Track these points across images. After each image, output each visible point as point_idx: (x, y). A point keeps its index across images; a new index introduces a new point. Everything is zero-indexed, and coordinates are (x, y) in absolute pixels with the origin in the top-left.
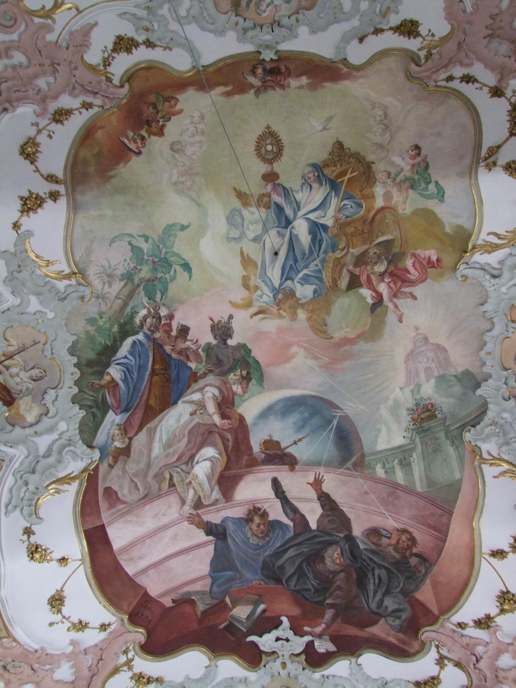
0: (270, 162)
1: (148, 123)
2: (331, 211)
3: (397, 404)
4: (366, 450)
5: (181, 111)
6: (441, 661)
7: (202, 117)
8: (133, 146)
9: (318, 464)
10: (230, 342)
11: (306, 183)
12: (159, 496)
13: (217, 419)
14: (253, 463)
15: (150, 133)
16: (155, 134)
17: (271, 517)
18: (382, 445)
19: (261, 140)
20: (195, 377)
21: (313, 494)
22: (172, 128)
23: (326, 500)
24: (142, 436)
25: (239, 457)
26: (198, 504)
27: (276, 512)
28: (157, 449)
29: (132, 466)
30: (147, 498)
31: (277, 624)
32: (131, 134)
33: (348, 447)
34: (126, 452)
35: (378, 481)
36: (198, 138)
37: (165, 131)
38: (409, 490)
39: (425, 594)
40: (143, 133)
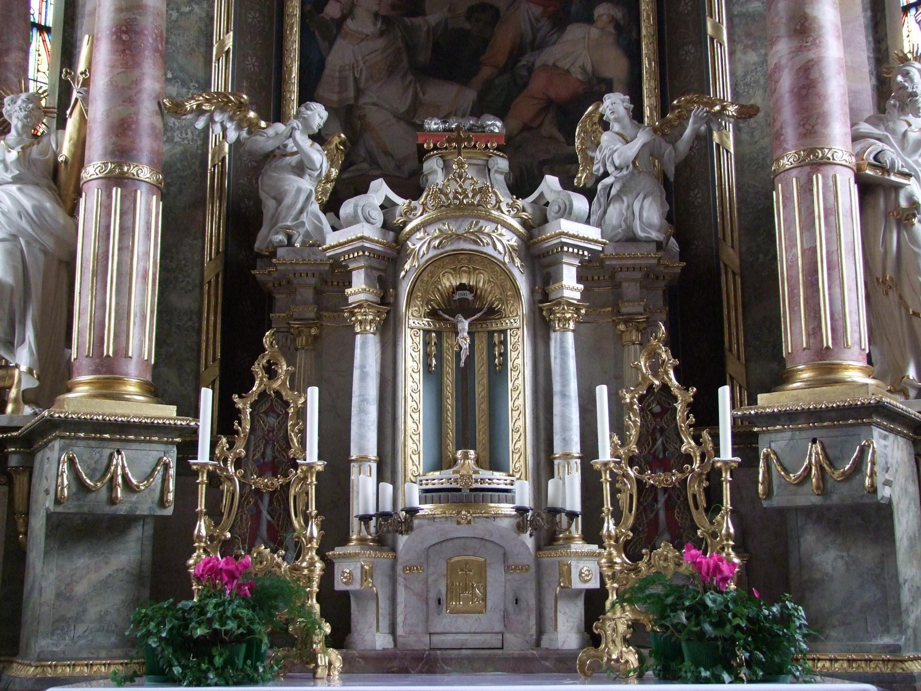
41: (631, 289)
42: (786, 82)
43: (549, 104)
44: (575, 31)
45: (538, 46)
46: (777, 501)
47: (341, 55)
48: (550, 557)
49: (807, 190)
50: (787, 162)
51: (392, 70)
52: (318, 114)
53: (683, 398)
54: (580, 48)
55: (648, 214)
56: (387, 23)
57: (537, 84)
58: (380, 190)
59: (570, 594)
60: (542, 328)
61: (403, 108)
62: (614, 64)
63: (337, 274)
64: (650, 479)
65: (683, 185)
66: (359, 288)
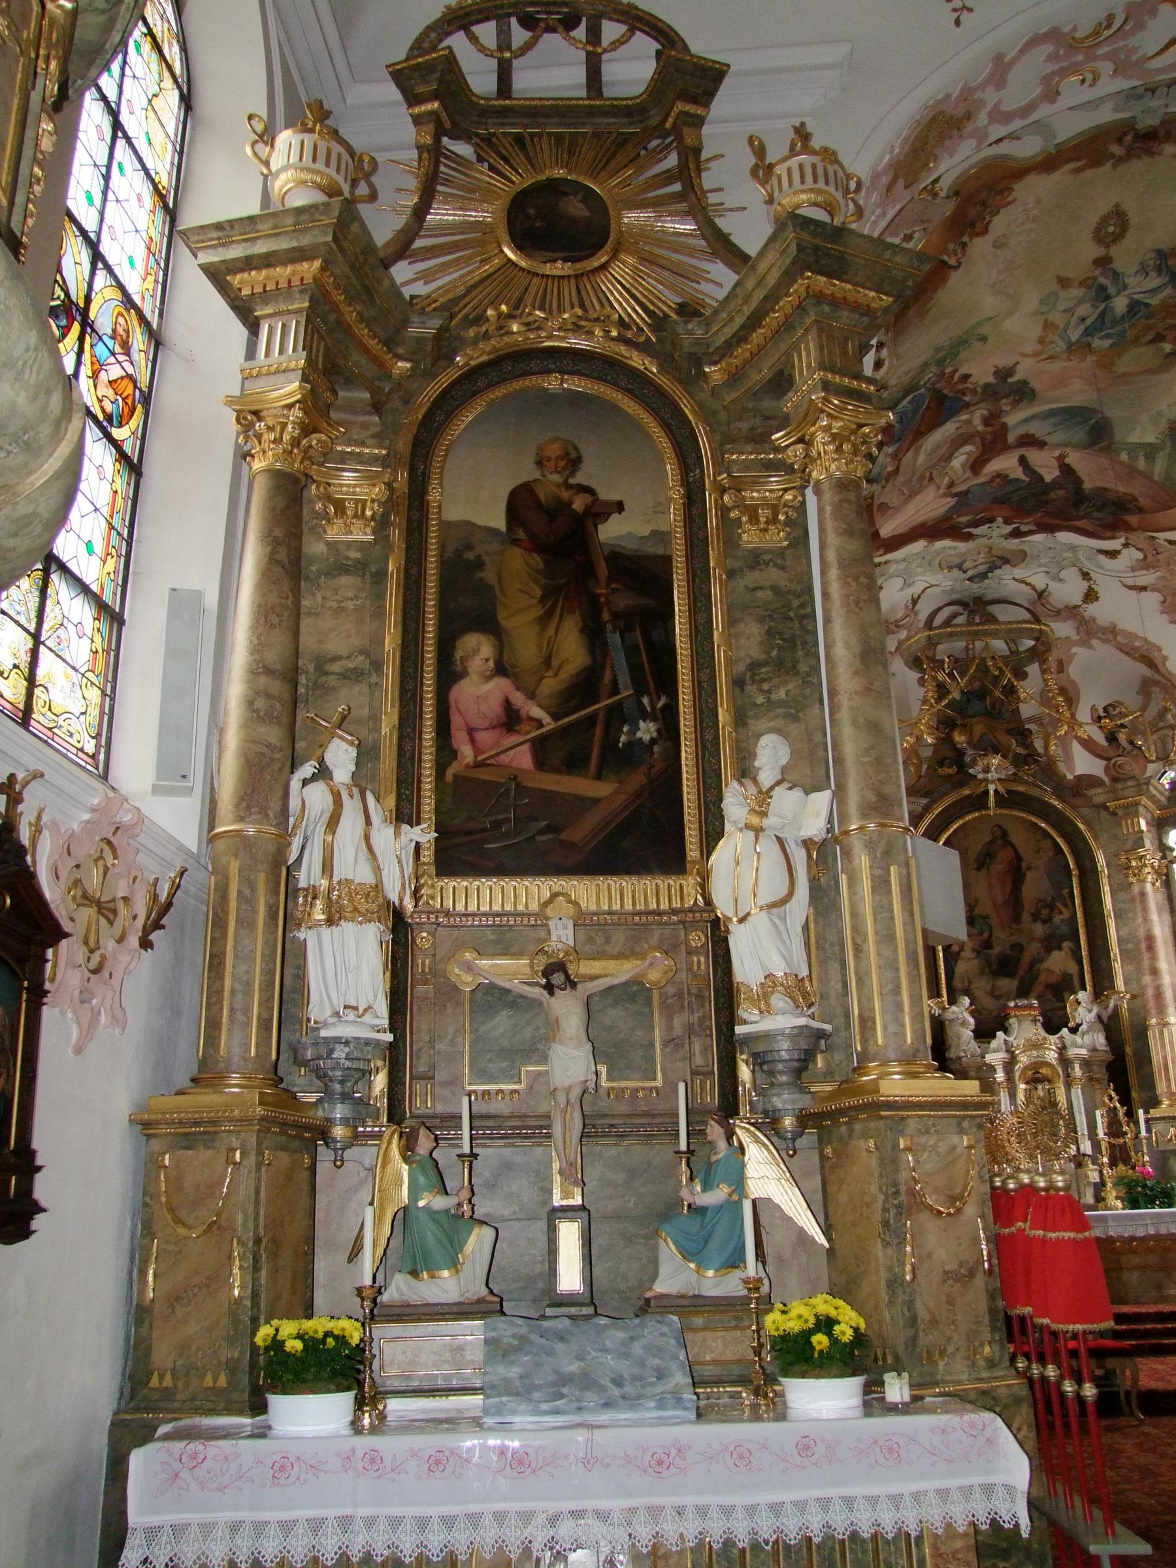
0: (1107, 246)
1: (972, 225)
2: (1161, 296)
3: (1160, 414)
4: (1117, 437)
5: (1014, 200)
6: (1126, 545)
7: (1038, 201)
8: (952, 261)
9: (1066, 445)
10: (1010, 380)
11: (1143, 270)
12: (920, 491)
13: (980, 428)
14: (1006, 448)
15: (972, 236)
16: (978, 235)
17: (1012, 476)
18: (1134, 438)
19: (1105, 220)
20: (967, 405)
21: (1055, 463)
22: (999, 224)
23: (1066, 470)
24: (910, 454)
25: (994, 442)
26: (952, 484)
27: (1018, 473)
28: (922, 458)
29: (900, 479)
30: (913, 494)
31: (991, 520)
32: (951, 246)
33: (1099, 433)
34: (896, 471)
35: (1122, 464)
36: (1027, 226)
37: (991, 227)
38: (1147, 477)
39: (1133, 520)
40: (965, 239)
41: (1095, 1068)
42: (1150, 992)
43: (1049, 986)
44: (1055, 954)
45: (1041, 961)
46: (1161, 1148)
47: (961, 967)
48: (1080, 1171)
49: (1162, 1033)
50: (1153, 1021)
51: (982, 974)
52: (966, 1001)
53: (1121, 1111)
54: (1058, 962)
55: (1100, 1040)
56: (978, 953)
57: (1042, 978)
58: (1000, 1034)
59: (1089, 1183)
60: (1068, 1086)
61: (989, 988)
62: (1073, 968)
63: (992, 1069)
64: (1113, 1141)
65: (1110, 1025)
66: (1000, 1076)
